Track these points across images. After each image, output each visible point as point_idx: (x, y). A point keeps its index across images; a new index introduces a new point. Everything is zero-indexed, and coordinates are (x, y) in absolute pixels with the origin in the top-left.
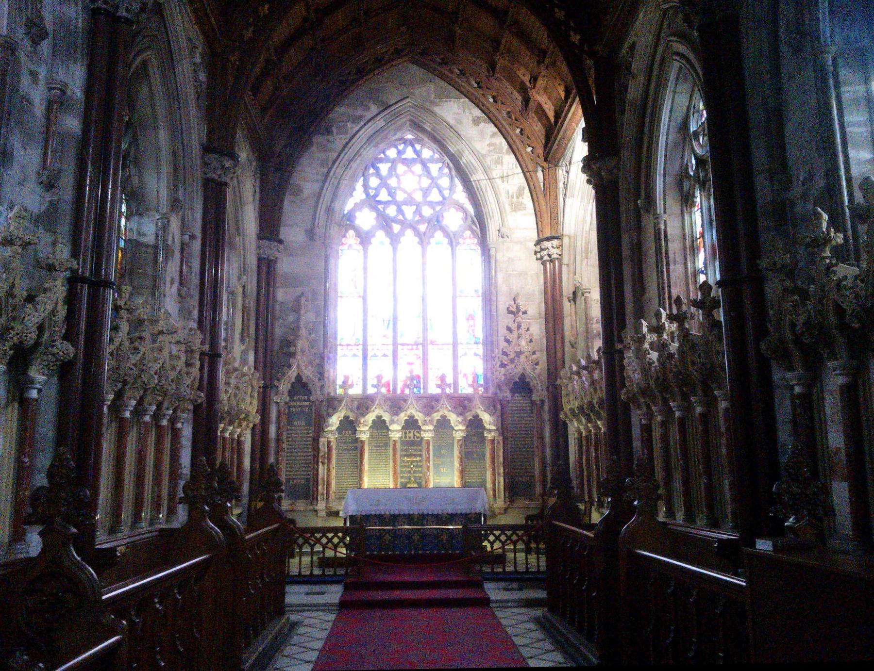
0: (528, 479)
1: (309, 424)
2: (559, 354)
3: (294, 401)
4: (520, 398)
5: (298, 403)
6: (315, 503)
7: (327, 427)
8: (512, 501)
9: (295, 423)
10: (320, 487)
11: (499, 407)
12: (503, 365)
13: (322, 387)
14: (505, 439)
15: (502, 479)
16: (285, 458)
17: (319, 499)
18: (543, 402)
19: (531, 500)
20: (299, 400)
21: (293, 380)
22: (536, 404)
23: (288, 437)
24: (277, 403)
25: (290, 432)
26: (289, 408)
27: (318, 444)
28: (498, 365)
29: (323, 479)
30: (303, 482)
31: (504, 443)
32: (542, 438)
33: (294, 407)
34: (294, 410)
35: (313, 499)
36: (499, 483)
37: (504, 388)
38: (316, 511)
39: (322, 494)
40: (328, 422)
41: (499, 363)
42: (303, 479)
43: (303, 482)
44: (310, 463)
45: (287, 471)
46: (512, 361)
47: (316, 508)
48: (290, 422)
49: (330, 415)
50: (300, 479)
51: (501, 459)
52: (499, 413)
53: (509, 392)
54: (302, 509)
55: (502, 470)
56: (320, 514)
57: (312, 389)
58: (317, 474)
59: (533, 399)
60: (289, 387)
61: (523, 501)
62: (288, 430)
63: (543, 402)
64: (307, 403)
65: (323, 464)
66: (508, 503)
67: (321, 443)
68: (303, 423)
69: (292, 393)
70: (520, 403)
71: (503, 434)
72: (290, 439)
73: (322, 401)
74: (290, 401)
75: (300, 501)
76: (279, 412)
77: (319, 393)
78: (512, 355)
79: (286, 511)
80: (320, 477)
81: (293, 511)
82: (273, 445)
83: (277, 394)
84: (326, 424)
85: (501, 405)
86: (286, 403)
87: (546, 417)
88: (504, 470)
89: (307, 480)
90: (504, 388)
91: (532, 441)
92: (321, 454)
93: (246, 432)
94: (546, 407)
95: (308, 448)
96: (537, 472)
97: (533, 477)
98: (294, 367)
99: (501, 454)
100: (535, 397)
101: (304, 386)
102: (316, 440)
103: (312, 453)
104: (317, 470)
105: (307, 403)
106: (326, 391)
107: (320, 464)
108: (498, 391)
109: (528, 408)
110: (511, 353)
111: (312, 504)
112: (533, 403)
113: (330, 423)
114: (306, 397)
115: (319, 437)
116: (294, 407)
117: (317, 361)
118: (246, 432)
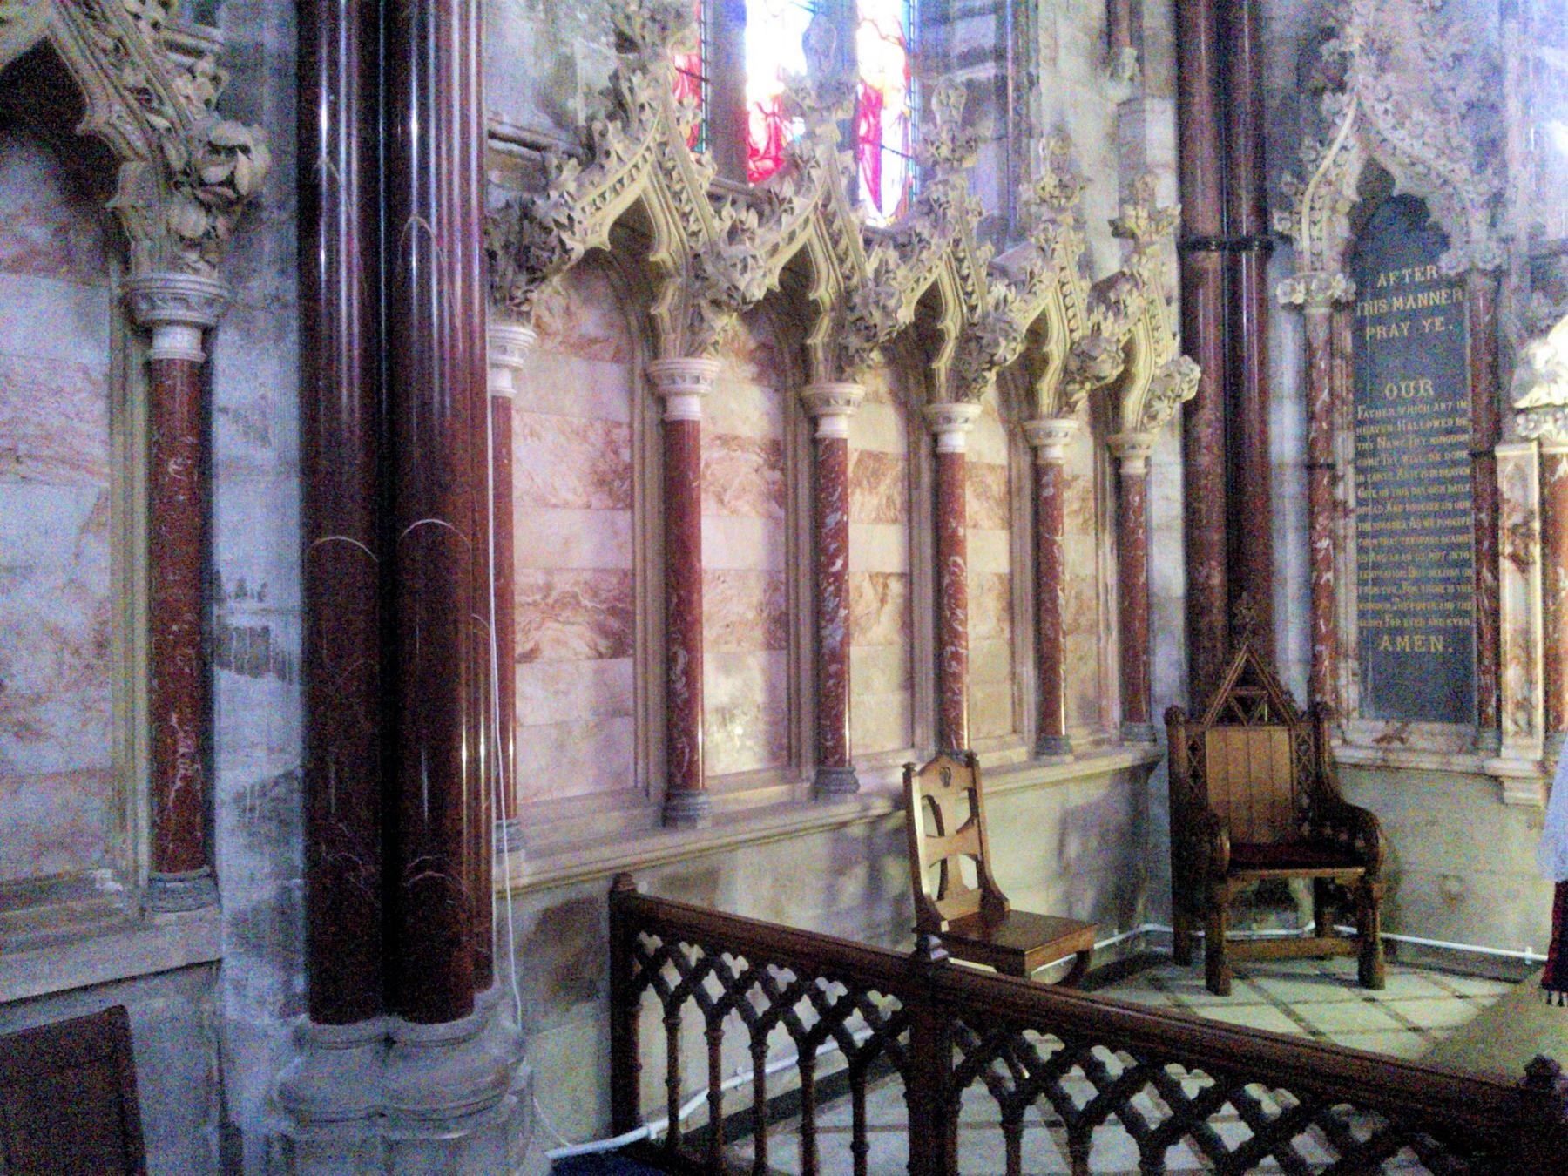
1: (1448, 389)
3: (1377, 295)
5: (1398, 303)
6: (1489, 738)
7: (1525, 389)
9: (1390, 390)
10: (1512, 675)
13: (1497, 200)
16: (1351, 546)
17: (1507, 724)
20: (1400, 288)
21: (1350, 193)
23: (1360, 454)
24: (1299, 309)
25: (1369, 430)
26: (1359, 326)
27: (1493, 471)
29: (1526, 632)
30: (1436, 643)
33: (1379, 320)
34: (1380, 331)
35: (1483, 723)
38: (1496, 779)
39: (1525, 705)
40: (1528, 362)
42: (1438, 630)
43: (1436, 643)
44: (1465, 563)
45: (1362, 598)
47: (1495, 766)
48: (1364, 390)
49: (1537, 330)
50: (1427, 632)
54: (1428, 763)
56: (1513, 793)
57: (1448, 224)
58: (1495, 613)
60: (1343, 228)
62: (1360, 423)
64: (1439, 297)
65: (1522, 564)
67: (1505, 471)
68: (1427, 386)
69: (1356, 258)
72: (1370, 462)
73: (1498, 275)
74: (1360, 294)
75: (1426, 727)
76: (1308, 348)
77: (1479, 230)
79: (1357, 766)
80: (1508, 628)
81: (1384, 767)
82: (1288, 491)
83: (1291, 271)
84: (1520, 374)
86: (1337, 305)
89: (1458, 638)
92: (1509, 520)
93: (1142, 437)
95: (1456, 498)
98: (1344, 130)
101: (1413, 209)
102: (1484, 458)
103: (1470, 521)
104: (1495, 595)
105: (1439, 297)
106: (1518, 219)
107: (1506, 565)
111: (1475, 747)
113: (1539, 364)
114: (1431, 271)
115: (1497, 434)
116: (1379, 320)
117: (1469, 87)
118: (1142, 437)
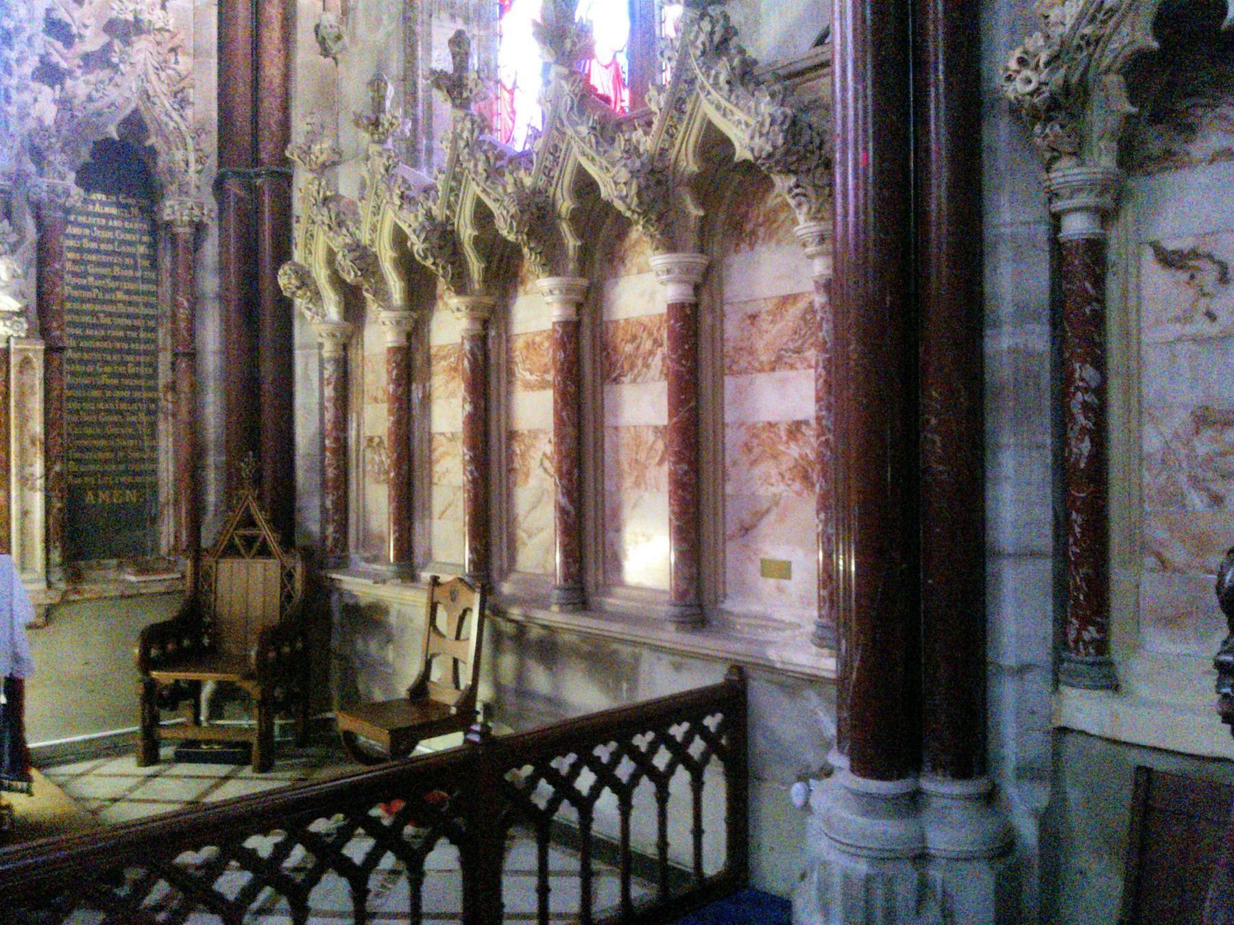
0: (131, 496)
2: (272, 71)
4: (114, 211)
8: (75, 577)
11: (30, 224)
12: (49, 73)
14: (52, 351)
15: (37, 502)
18: (199, 228)
19: (143, 570)
22: (174, 239)
28: (28, 69)
31: (47, 364)
32: (189, 354)
36: (25, 514)
37: (57, 159)
41: (33, 62)
46: (91, 61)
51: (37, 427)
52: (28, 248)
53: (72, 176)
55: (38, 468)
59: (167, 215)
61: (112, 575)
63: (199, 228)
66: (62, 586)
70: (106, 228)
71: (44, 332)
78: (93, 41)
85: (38, 217)
87: (210, 283)
88: (48, 469)
90: (57, 159)
91: (153, 366)
94: (210, 249)
96: (167, 467)
97: (154, 488)
99: (36, 405)
100: (173, 209)
108: (31, 168)
109: (142, 249)
110: (87, 33)
112: (158, 230)
